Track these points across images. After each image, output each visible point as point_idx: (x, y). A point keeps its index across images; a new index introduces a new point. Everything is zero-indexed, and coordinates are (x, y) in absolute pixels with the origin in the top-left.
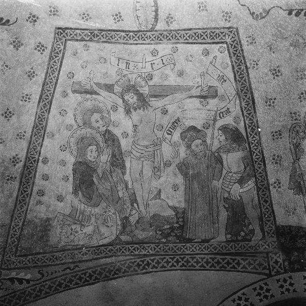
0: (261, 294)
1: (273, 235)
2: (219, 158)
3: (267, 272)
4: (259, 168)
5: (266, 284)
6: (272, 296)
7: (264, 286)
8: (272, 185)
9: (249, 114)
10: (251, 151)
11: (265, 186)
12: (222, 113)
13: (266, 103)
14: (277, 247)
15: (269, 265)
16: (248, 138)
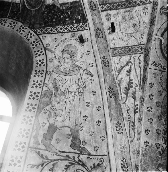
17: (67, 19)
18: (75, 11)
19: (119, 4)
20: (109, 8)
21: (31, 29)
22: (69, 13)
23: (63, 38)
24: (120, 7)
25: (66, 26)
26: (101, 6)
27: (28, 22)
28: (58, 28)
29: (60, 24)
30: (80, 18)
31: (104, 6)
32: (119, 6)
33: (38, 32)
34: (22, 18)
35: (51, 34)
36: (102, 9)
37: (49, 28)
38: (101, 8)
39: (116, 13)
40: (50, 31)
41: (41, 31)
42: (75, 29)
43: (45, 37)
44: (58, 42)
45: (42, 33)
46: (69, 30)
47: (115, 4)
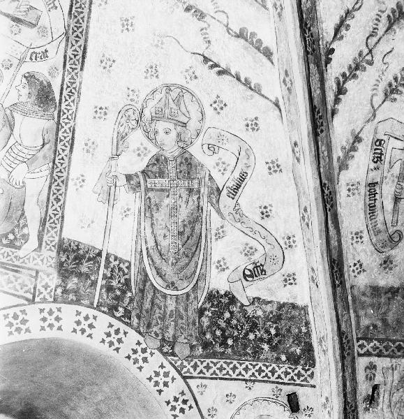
0: (13, 325)
1: (53, 248)
2: (10, 118)
3: (30, 297)
4: (63, 150)
5: (23, 312)
6: (28, 330)
7: (19, 314)
8: (73, 180)
9: (73, 69)
10: (58, 123)
11: (62, 179)
12: (36, 53)
13: (102, 62)
14: (53, 266)
15: (35, 288)
16: (60, 103)
17: (266, 347)
18: (289, 331)
19: (400, 345)
20: (378, 351)
21: (165, 354)
22: (273, 332)
23: (251, 395)
24: (399, 354)
25: (260, 364)
26: (361, 342)
27: (157, 335)
28: (238, 365)
29: (246, 354)
30: (298, 351)
31: (365, 343)
32: (399, 351)
33: (185, 370)
34: (139, 317)
35: (221, 379)
36: (360, 350)
37: (215, 361)
38: (359, 346)
39: (390, 365)
40: (218, 372)
41: (195, 367)
42: (283, 376)
43: (206, 386)
44: (237, 404)
45: (195, 374)
46: (267, 375)
47: (390, 344)
